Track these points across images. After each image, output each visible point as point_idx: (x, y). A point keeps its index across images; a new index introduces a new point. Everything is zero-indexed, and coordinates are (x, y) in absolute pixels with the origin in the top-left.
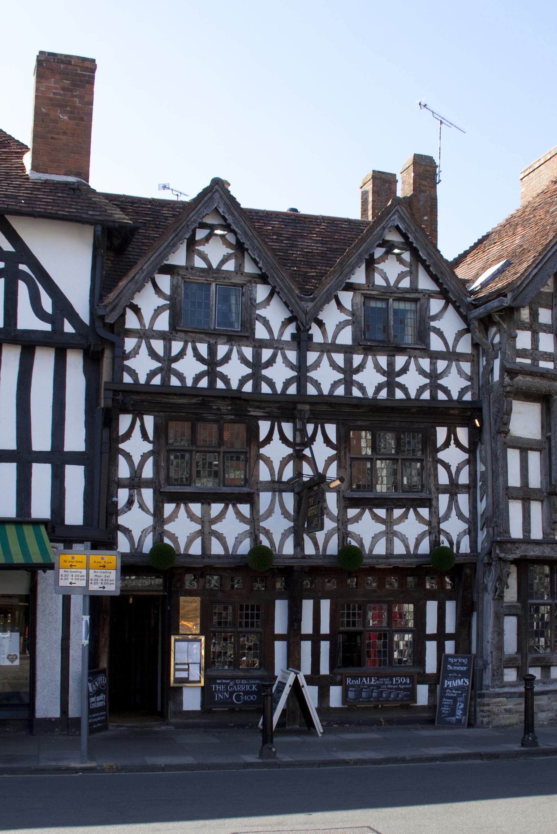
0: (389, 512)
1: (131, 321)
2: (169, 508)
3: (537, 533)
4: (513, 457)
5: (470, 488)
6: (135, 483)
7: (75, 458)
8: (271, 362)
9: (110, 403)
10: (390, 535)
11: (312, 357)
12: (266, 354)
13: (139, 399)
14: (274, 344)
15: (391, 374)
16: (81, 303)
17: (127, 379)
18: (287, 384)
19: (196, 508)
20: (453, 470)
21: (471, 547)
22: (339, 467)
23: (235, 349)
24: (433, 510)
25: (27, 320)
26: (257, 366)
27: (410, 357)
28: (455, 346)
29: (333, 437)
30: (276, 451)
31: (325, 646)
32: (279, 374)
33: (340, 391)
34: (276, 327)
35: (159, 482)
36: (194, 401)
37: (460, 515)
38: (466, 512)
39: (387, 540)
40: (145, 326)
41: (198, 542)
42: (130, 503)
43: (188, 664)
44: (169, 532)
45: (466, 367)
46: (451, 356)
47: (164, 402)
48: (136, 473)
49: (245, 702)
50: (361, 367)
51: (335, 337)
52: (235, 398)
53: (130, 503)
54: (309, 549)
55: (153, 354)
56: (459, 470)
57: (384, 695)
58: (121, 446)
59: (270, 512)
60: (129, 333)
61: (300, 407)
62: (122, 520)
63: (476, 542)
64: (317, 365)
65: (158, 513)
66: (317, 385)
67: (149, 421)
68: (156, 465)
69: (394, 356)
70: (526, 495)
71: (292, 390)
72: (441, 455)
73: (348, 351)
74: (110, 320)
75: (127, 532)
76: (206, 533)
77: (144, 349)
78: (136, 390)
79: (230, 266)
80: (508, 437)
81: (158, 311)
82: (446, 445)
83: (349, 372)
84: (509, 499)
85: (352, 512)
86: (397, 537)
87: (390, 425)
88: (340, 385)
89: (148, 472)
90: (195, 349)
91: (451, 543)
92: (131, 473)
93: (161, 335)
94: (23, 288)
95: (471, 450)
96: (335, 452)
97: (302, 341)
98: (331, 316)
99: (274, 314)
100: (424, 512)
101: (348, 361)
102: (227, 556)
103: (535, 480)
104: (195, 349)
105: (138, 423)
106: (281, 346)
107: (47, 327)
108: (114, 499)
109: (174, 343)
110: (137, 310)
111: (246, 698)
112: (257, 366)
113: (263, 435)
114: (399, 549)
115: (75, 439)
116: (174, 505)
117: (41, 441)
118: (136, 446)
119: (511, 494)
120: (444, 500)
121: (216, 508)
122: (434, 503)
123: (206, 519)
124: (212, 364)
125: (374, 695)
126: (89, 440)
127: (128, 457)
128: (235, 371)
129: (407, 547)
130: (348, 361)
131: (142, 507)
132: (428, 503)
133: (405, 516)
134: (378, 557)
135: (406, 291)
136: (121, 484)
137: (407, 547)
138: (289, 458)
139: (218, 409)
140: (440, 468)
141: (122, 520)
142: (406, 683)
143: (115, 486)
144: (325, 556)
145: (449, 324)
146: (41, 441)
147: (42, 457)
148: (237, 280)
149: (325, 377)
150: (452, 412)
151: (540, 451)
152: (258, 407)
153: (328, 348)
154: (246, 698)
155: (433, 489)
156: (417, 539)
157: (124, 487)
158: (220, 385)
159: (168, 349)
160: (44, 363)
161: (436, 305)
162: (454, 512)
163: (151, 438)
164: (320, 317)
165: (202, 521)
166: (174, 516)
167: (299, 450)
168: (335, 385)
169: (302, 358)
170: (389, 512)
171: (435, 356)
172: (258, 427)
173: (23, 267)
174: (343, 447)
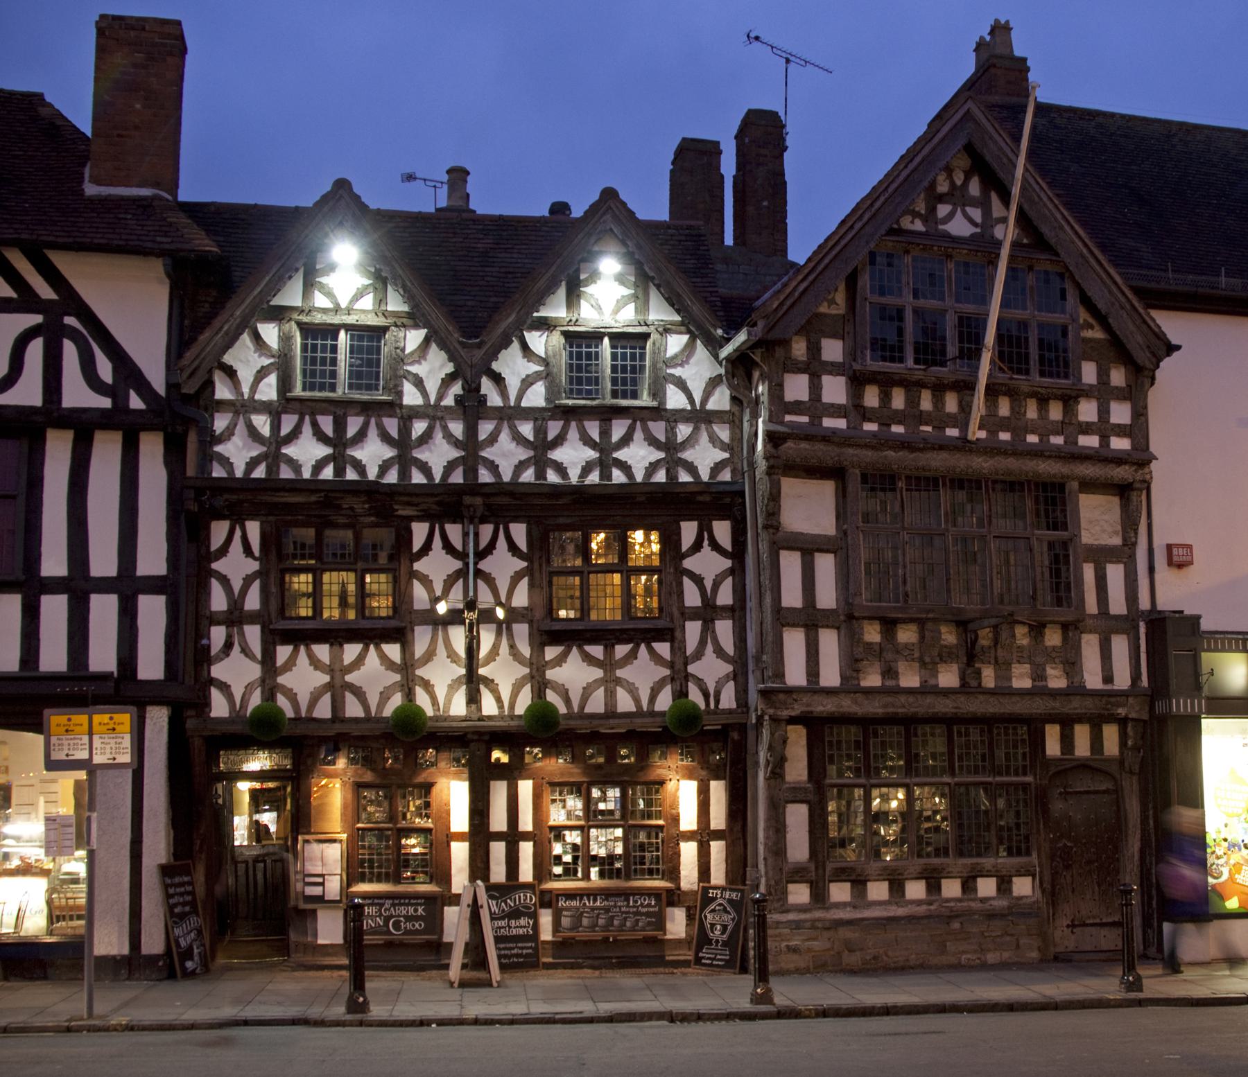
0: (609, 649)
1: (223, 392)
2: (283, 652)
3: (830, 676)
4: (791, 563)
5: (737, 612)
6: (235, 617)
7: (154, 585)
8: (426, 438)
9: (201, 504)
10: (611, 683)
11: (485, 429)
13: (240, 498)
17: (218, 472)
18: (450, 467)
19: (322, 651)
20: (708, 584)
21: (737, 700)
22: (531, 586)
23: (373, 421)
24: (676, 645)
25: (77, 394)
26: (403, 445)
27: (635, 421)
28: (705, 400)
29: (522, 543)
32: (438, 456)
33: (528, 476)
34: (432, 387)
35: (269, 615)
36: (313, 498)
37: (720, 652)
38: (730, 649)
39: (606, 691)
40: (242, 395)
41: (326, 699)
42: (228, 646)
43: (323, 876)
44: (283, 686)
45: (724, 433)
46: (700, 417)
48: (236, 603)
49: (407, 932)
51: (520, 397)
52: (371, 491)
53: (228, 646)
56: (716, 585)
57: (616, 922)
58: (214, 566)
61: (468, 500)
62: (217, 671)
63: (746, 691)
64: (493, 439)
65: (268, 660)
66: (493, 468)
67: (254, 529)
68: (264, 591)
69: (610, 420)
72: (688, 563)
74: (189, 389)
75: (225, 688)
77: (241, 428)
78: (231, 485)
80: (780, 534)
81: (261, 374)
82: (697, 547)
83: (541, 448)
84: (783, 626)
85: (551, 652)
86: (622, 686)
87: (608, 522)
88: (526, 469)
89: (253, 602)
90: (315, 425)
92: (229, 605)
93: (265, 407)
94: (70, 350)
95: (737, 554)
96: (525, 564)
98: (513, 366)
100: (663, 648)
101: (540, 431)
102: (368, 719)
104: (315, 425)
105: (238, 533)
106: (439, 414)
107: (106, 403)
108: (204, 642)
109: (284, 417)
110: (231, 373)
111: (409, 925)
113: (417, 544)
114: (625, 703)
115: (153, 559)
116: (290, 648)
117: (104, 563)
118: (236, 566)
119: (784, 618)
120: (693, 630)
121: (351, 651)
122: (678, 634)
123: (337, 667)
125: (601, 922)
127: (225, 581)
128: (372, 454)
129: (637, 701)
131: (246, 651)
132: (669, 633)
133: (633, 655)
134: (593, 716)
136: (214, 620)
137: (637, 701)
139: (352, 509)
140: (688, 583)
141: (217, 671)
142: (649, 905)
143: (207, 622)
144: (512, 717)
146: (104, 563)
147: (104, 585)
149: (506, 456)
150: (700, 498)
151: (835, 552)
152: (409, 504)
153: (511, 414)
154: (409, 925)
155: (676, 613)
156: (652, 689)
157: (219, 623)
158: (351, 475)
160: (106, 455)
163: (257, 554)
164: (495, 366)
165: (330, 670)
166: (290, 664)
168: (520, 467)
169: (471, 431)
170: (609, 649)
172: (410, 533)
173: (70, 321)
174: (536, 557)
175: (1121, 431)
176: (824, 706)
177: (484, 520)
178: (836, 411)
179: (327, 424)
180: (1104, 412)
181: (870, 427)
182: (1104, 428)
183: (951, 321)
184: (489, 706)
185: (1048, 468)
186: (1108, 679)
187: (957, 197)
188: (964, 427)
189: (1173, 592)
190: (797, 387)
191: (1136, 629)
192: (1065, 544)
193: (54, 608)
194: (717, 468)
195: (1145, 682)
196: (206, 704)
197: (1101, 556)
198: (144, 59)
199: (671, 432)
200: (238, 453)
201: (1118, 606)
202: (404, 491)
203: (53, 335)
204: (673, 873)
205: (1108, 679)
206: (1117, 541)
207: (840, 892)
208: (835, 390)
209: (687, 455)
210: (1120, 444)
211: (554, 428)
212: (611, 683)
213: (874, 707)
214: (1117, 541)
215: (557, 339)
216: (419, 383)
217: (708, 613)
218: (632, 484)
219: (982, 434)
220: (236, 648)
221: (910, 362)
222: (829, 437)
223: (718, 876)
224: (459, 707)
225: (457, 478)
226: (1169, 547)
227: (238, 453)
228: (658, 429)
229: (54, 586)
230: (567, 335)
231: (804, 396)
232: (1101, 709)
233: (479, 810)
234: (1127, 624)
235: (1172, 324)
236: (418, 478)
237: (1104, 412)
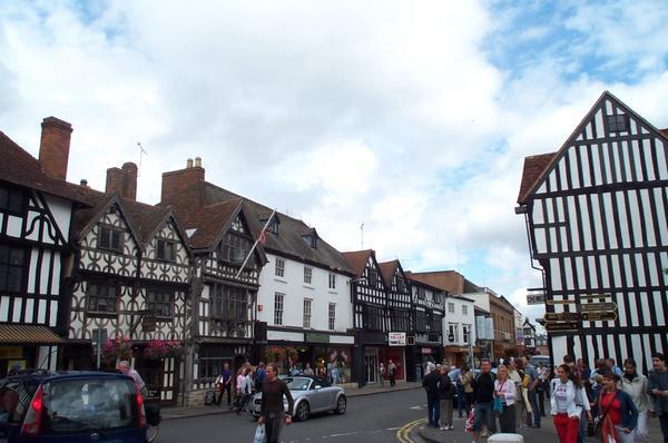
2: (89, 320)
4: (201, 305)
6: (78, 309)
7: (54, 298)
12: (127, 260)
19: (98, 320)
25: (47, 239)
30: (126, 298)
33: (149, 277)
46: (182, 266)
47: (94, 277)
48: (78, 305)
52: (116, 277)
54: (134, 338)
60: (82, 248)
62: (72, 325)
65: (85, 323)
67: (85, 284)
70: (204, 319)
71: (135, 275)
73: (152, 261)
79: (117, 224)
81: (93, 240)
89: (82, 305)
94: (46, 224)
97: (139, 256)
98: (149, 248)
99: (130, 245)
107: (53, 242)
115: (55, 291)
117: (43, 291)
120: (176, 319)
121: (105, 320)
124: (110, 262)
131: (80, 320)
132: (171, 320)
141: (72, 325)
145: (182, 254)
146: (43, 291)
147: (43, 297)
153: (147, 260)
159: (95, 255)
161: (179, 246)
167: (134, 296)
169: (139, 263)
171: (178, 265)
179: (107, 256)
185: (246, 286)
193: (30, 303)
202: (123, 278)
203: (42, 219)
208: (215, 265)
211: (155, 265)
227: (86, 261)
229: (31, 296)
236: (126, 275)
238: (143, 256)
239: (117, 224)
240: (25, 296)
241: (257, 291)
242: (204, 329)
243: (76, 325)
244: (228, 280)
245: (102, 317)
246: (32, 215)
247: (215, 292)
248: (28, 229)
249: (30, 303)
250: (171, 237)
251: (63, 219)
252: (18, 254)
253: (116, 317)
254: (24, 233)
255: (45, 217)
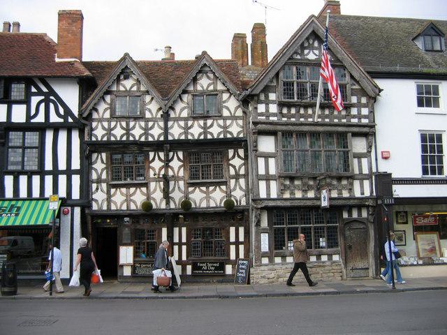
0: (207, 188)
2: (113, 191)
3: (274, 195)
4: (261, 161)
5: (246, 176)
6: (99, 181)
7: (76, 172)
9: (90, 149)
11: (170, 123)
13: (97, 147)
14: (154, 120)
15: (205, 128)
16: (75, 111)
17: (94, 139)
18: (159, 136)
19: (124, 190)
22: (184, 170)
25: (54, 119)
26: (146, 130)
29: (181, 157)
30: (157, 164)
31: (184, 248)
32: (156, 133)
33: (183, 137)
34: (154, 112)
37: (241, 188)
38: (244, 187)
42: (97, 189)
45: (240, 122)
47: (111, 147)
50: (192, 126)
51: (180, 114)
52: (135, 143)
55: (104, 128)
56: (240, 168)
59: (155, 190)
62: (94, 196)
64: (172, 127)
67: (104, 155)
68: (107, 172)
73: (186, 119)
75: (96, 201)
76: (128, 200)
77: (100, 126)
82: (234, 157)
83: (187, 128)
85: (191, 189)
89: (104, 176)
91: (237, 201)
94: (52, 106)
100: (224, 187)
101: (186, 124)
103: (272, 171)
104: (120, 124)
107: (62, 120)
112: (146, 130)
114: (212, 204)
115: (76, 165)
117: (62, 166)
120: (233, 182)
121: (132, 190)
124: (128, 130)
126: (81, 164)
127: (96, 170)
128: (137, 133)
129: (216, 204)
130: (186, 124)
132: (225, 183)
133: (215, 190)
135: (212, 91)
137: (216, 204)
138: (163, 167)
141: (94, 196)
146: (62, 166)
147: (62, 172)
148: (138, 94)
149: (176, 132)
157: (94, 183)
158: (131, 138)
159: (109, 125)
160: (63, 136)
162: (238, 187)
166: (115, 194)
168: (181, 134)
170: (207, 188)
171: (225, 119)
173: (52, 98)
175: (365, 117)
176: (271, 204)
177: (170, 151)
178: (274, 115)
179: (124, 124)
180: (359, 112)
181: (285, 119)
182: (360, 116)
183: (308, 85)
184: (172, 206)
185: (340, 129)
186: (363, 194)
187: (311, 48)
188: (314, 119)
189: (384, 167)
190: (261, 108)
191: (372, 178)
192: (348, 152)
193: (49, 179)
194: (239, 133)
195: (374, 194)
196: (90, 206)
197: (359, 156)
198: (72, 20)
199: (225, 123)
200: (99, 133)
201: (366, 171)
202: (147, 144)
203: (47, 102)
204: (229, 255)
205: (363, 194)
206: (365, 151)
207: (278, 260)
208: (273, 108)
209: (229, 130)
210: (365, 121)
212: (208, 198)
213: (288, 204)
214: (365, 151)
215: (190, 97)
216: (150, 111)
217: (237, 177)
218: (213, 139)
219: (320, 120)
220: (100, 190)
221: (296, 99)
222: (272, 123)
223: (242, 256)
224: (163, 206)
225: (162, 138)
226: (382, 152)
228: (221, 122)
229: (49, 173)
230: (193, 95)
231: (264, 111)
232: (360, 204)
233: (170, 236)
234: (369, 177)
235: (381, 83)
236: (150, 139)
237: (359, 112)
238: (172, 115)
239: (135, 88)
240: (42, 172)
241: (374, 134)
242: (269, 191)
243: (99, 198)
244: (302, 124)
245: (128, 186)
246: (35, 100)
247: (280, 144)
248: (33, 112)
249: (49, 179)
250: (211, 88)
251: (70, 95)
252: (32, 138)
253: (146, 185)
254: (29, 117)
255: (51, 98)
